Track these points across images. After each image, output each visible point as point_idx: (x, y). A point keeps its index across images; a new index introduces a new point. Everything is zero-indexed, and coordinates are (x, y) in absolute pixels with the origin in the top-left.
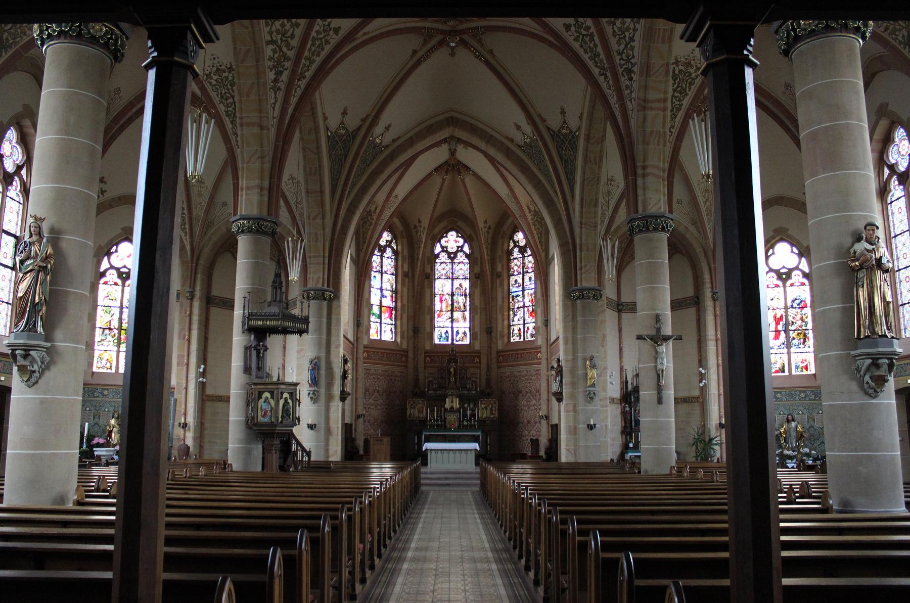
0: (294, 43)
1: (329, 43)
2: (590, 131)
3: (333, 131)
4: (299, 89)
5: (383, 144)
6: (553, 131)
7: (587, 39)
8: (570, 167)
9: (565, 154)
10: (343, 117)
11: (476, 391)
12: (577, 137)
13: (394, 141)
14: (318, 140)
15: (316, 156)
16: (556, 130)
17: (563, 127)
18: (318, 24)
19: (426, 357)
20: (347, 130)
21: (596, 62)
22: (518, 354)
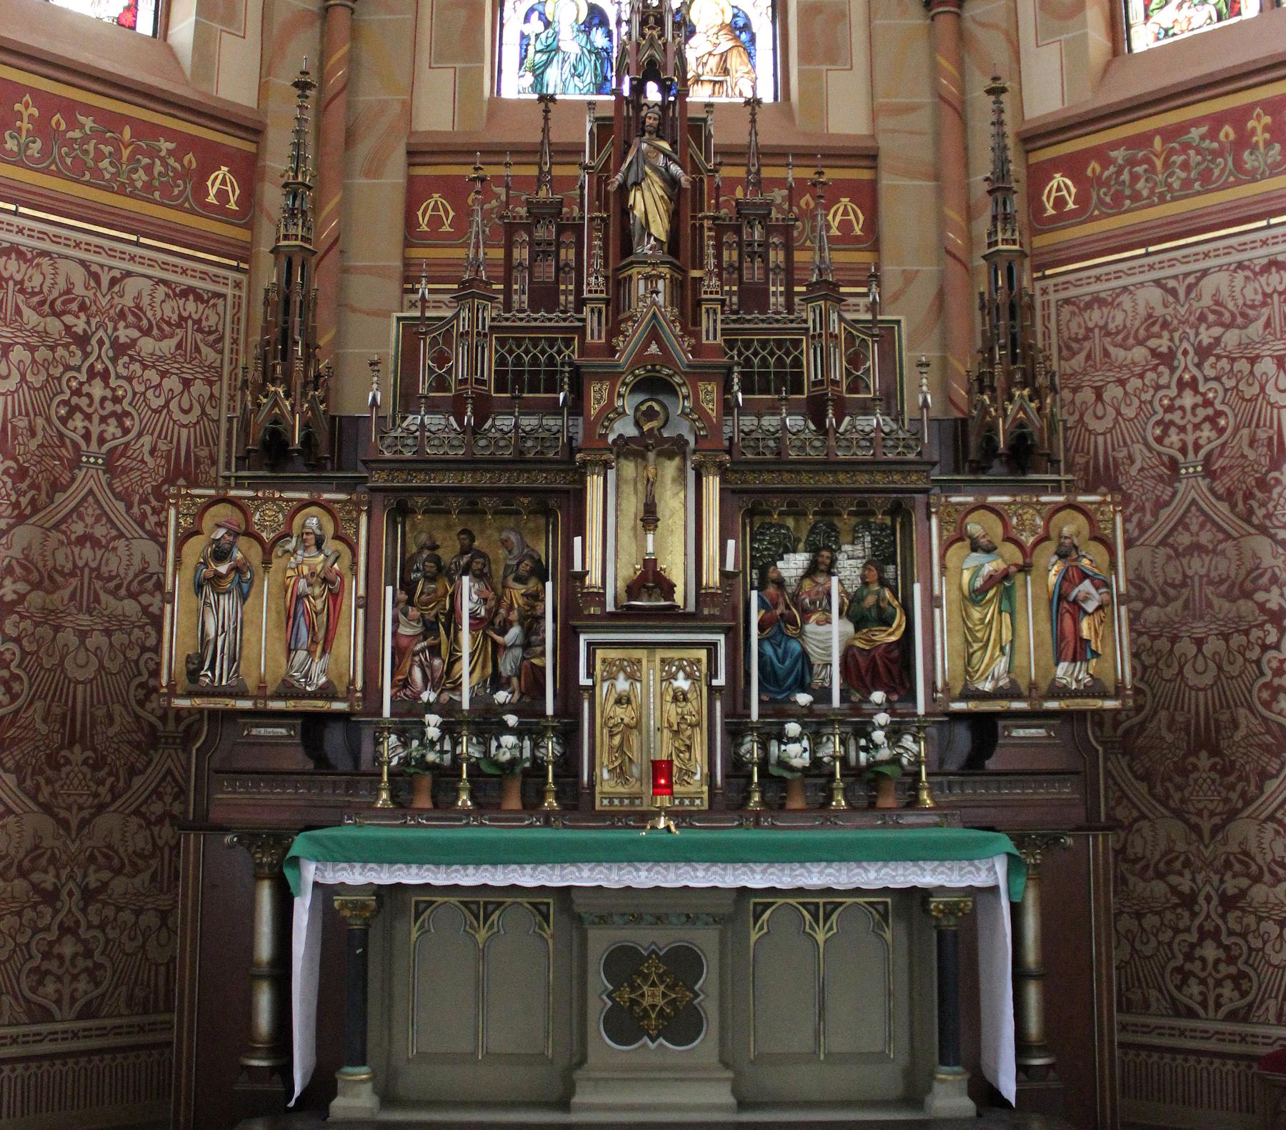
11: (890, 400)
19: (414, 195)
22: (1239, 117)
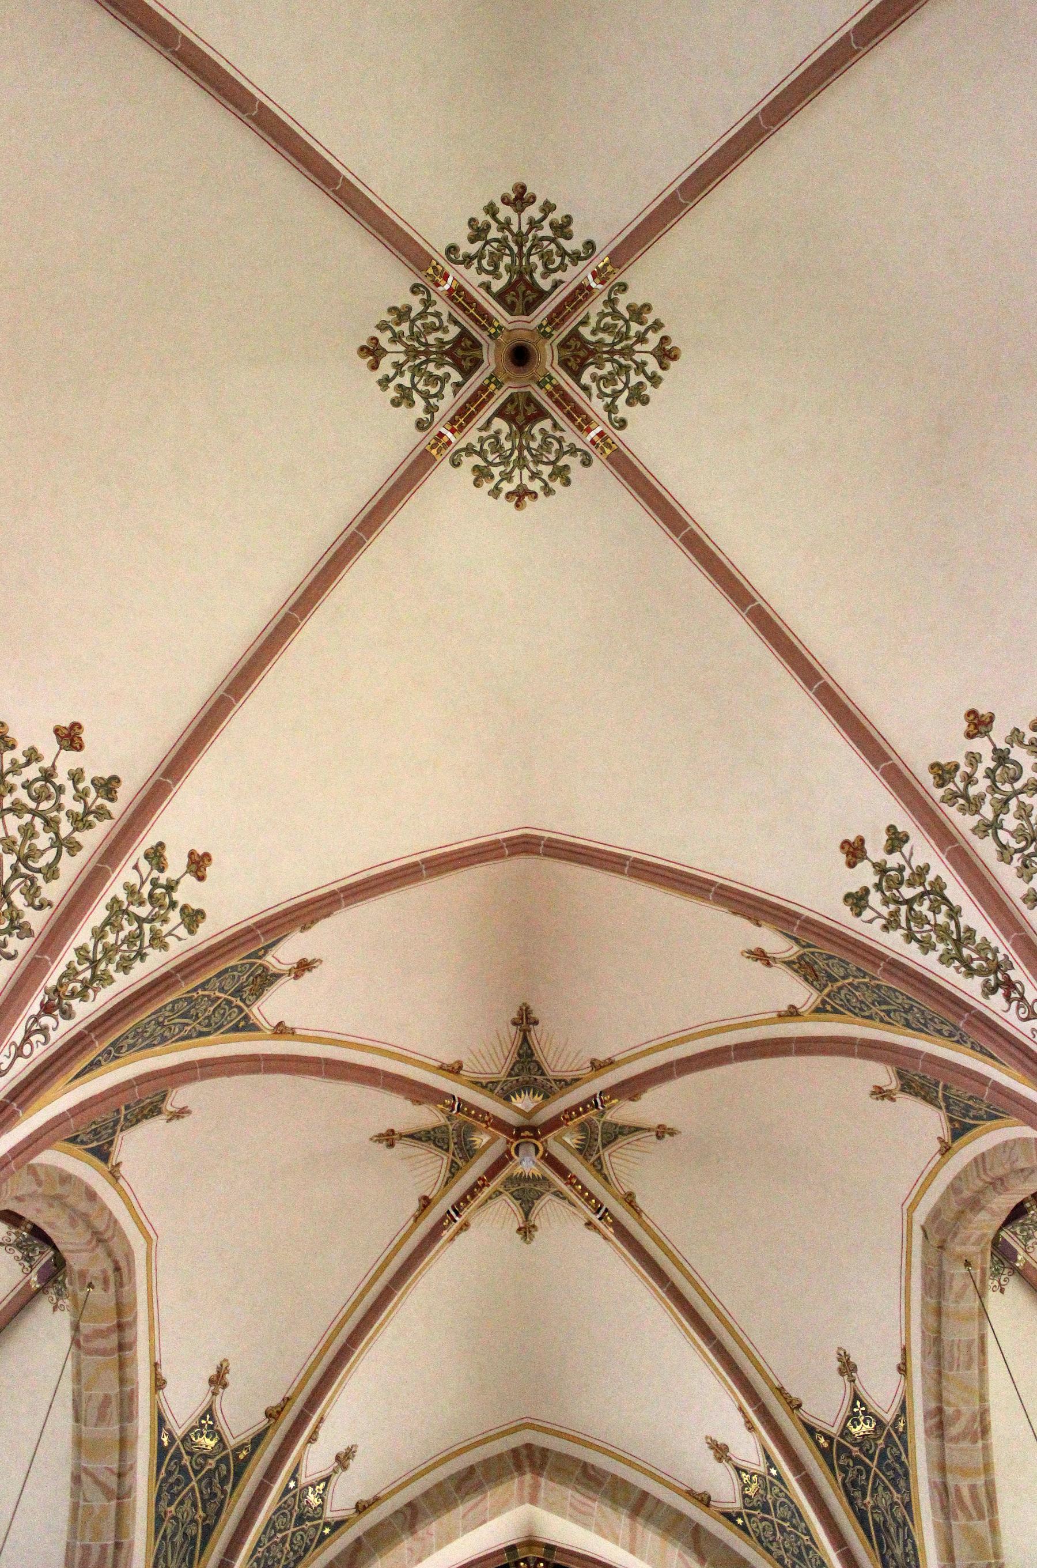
0: (53, 891)
1: (165, 947)
2: (939, 1398)
3: (179, 1433)
4: (40, 1037)
5: (329, 1515)
6: (828, 1438)
7: (923, 908)
8: (899, 1551)
9: (875, 1507)
10: (214, 1394)
12: (903, 1436)
13: (361, 1508)
14: (125, 1444)
15: (114, 1503)
16: (834, 1431)
17: (853, 1418)
18: (136, 867)
20: (221, 1440)
21: (966, 963)
